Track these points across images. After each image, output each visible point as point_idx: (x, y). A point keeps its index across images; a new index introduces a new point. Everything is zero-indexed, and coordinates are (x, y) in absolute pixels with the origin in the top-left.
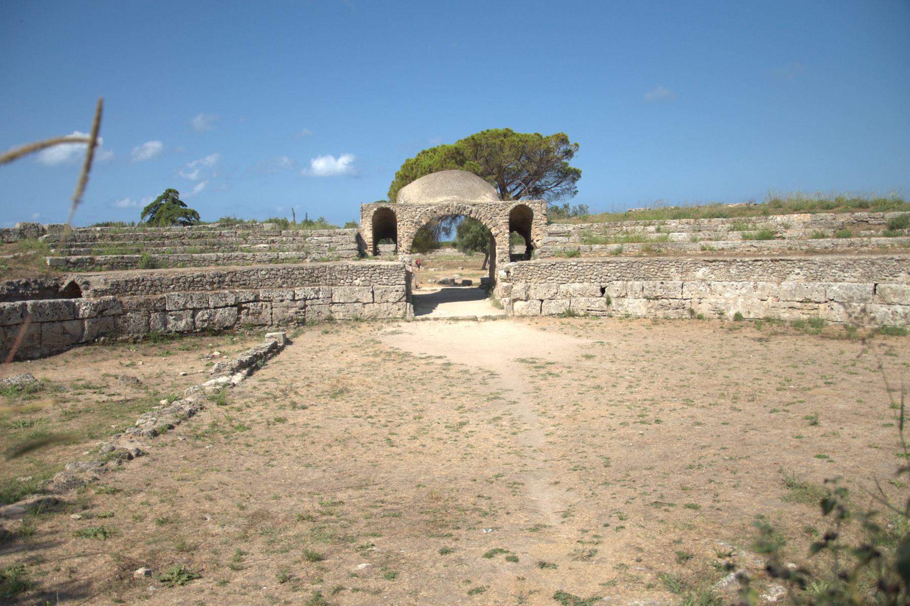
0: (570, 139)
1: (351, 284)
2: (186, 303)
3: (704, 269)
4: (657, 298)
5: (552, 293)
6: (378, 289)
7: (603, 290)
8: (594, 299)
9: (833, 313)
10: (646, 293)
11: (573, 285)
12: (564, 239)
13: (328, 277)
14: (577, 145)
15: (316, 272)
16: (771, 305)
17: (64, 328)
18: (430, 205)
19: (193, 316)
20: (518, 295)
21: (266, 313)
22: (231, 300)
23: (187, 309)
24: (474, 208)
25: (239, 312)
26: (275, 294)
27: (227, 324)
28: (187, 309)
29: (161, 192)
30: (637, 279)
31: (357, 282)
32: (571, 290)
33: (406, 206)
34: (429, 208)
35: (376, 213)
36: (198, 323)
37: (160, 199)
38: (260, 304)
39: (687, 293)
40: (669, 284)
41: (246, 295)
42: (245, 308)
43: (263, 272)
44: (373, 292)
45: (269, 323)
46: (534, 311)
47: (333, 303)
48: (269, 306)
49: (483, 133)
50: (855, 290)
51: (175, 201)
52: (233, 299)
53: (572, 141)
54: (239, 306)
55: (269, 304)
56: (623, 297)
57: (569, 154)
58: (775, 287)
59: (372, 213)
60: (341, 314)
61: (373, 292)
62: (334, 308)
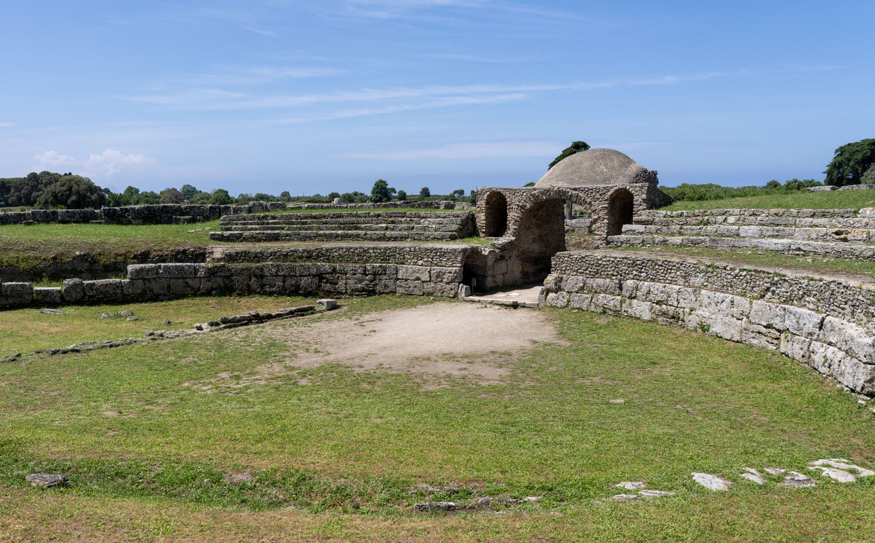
8: (611, 297)
17: (187, 283)
19: (284, 282)
21: (341, 283)
25: (320, 281)
32: (595, 285)
52: (315, 270)
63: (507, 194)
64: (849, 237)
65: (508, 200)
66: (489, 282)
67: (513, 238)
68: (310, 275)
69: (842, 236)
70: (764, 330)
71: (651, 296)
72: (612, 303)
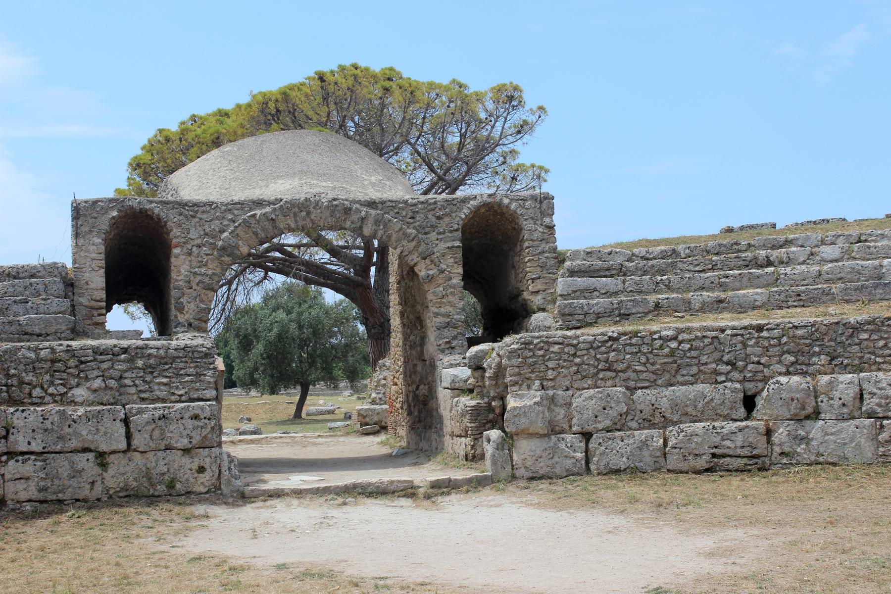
0: (526, 97)
1: (62, 399)
6: (140, 412)
7: (749, 403)
10: (871, 403)
18: (259, 203)
20: (524, 422)
24: (373, 212)
30: (844, 368)
31: (80, 393)
32: (664, 404)
33: (191, 209)
34: (258, 212)
35: (115, 223)
44: (126, 421)
49: (342, 68)
56: (808, 417)
57: (522, 129)
59: (104, 223)
60: (32, 485)
61: (126, 421)
63: (172, 218)
65: (176, 232)
71: (871, 403)
72: (739, 439)
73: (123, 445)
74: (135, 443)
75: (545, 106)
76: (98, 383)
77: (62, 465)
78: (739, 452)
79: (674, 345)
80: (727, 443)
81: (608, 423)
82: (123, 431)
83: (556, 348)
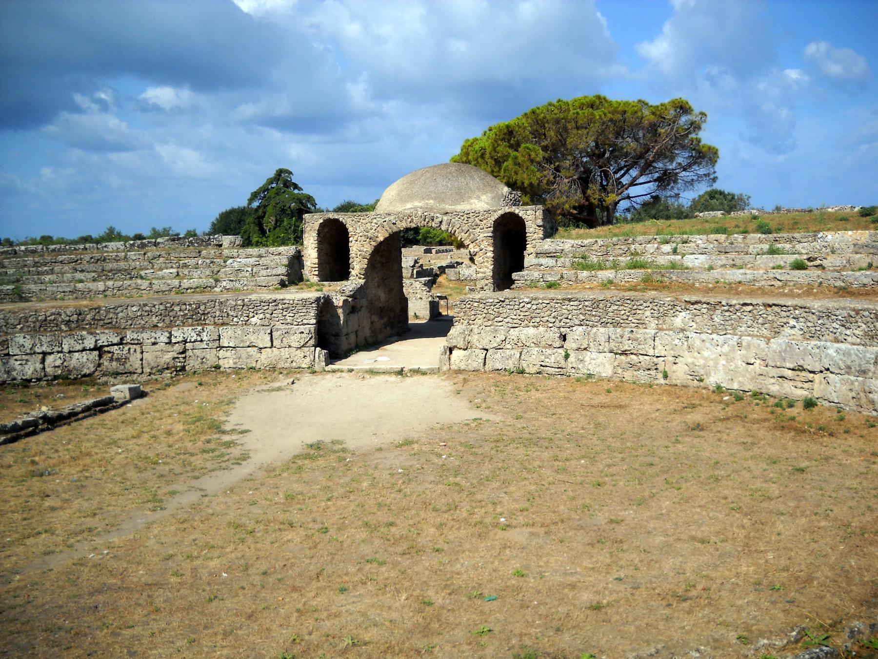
2: (34, 345)
3: (683, 314)
4: (624, 353)
5: (498, 340)
6: (277, 330)
8: (549, 351)
9: (830, 388)
10: (612, 344)
11: (525, 330)
12: (550, 262)
13: (218, 313)
14: (703, 114)
15: (202, 307)
16: (758, 371)
18: (389, 215)
22: (90, 342)
23: (34, 353)
24: (445, 218)
25: (100, 356)
26: (145, 336)
27: (86, 371)
28: (34, 353)
29: (272, 174)
30: (605, 324)
31: (254, 320)
32: (523, 337)
36: (48, 370)
37: (270, 181)
38: (127, 348)
39: (660, 347)
40: (640, 333)
41: (106, 337)
42: (109, 352)
43: (134, 309)
44: (271, 333)
45: (139, 371)
46: (475, 365)
47: (221, 347)
48: (139, 350)
50: (854, 357)
51: (288, 184)
53: (696, 109)
54: (99, 349)
55: (138, 348)
56: (585, 349)
58: (763, 344)
60: (231, 362)
62: (222, 353)
64: (825, 263)
65: (350, 229)
66: (344, 343)
67: (362, 281)
68: (84, 350)
69: (818, 262)
70: (789, 373)
72: (553, 359)
73: (269, 345)
74: (274, 344)
75: (704, 111)
76: (261, 316)
77: (243, 352)
78: (553, 365)
79: (529, 306)
80: (547, 360)
81: (496, 345)
82: (269, 338)
83: (476, 304)
